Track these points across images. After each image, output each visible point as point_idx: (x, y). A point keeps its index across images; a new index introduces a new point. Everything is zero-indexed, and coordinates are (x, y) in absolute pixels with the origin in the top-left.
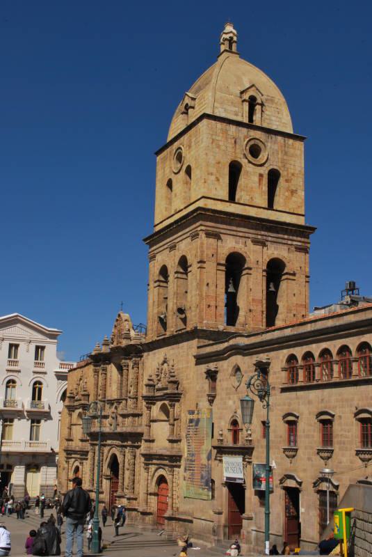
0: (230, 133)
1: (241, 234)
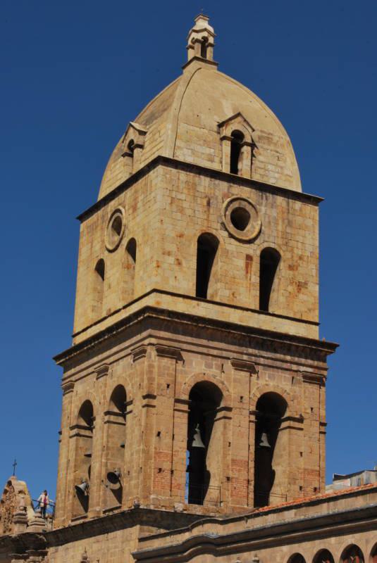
0: (201, 189)
1: (215, 352)
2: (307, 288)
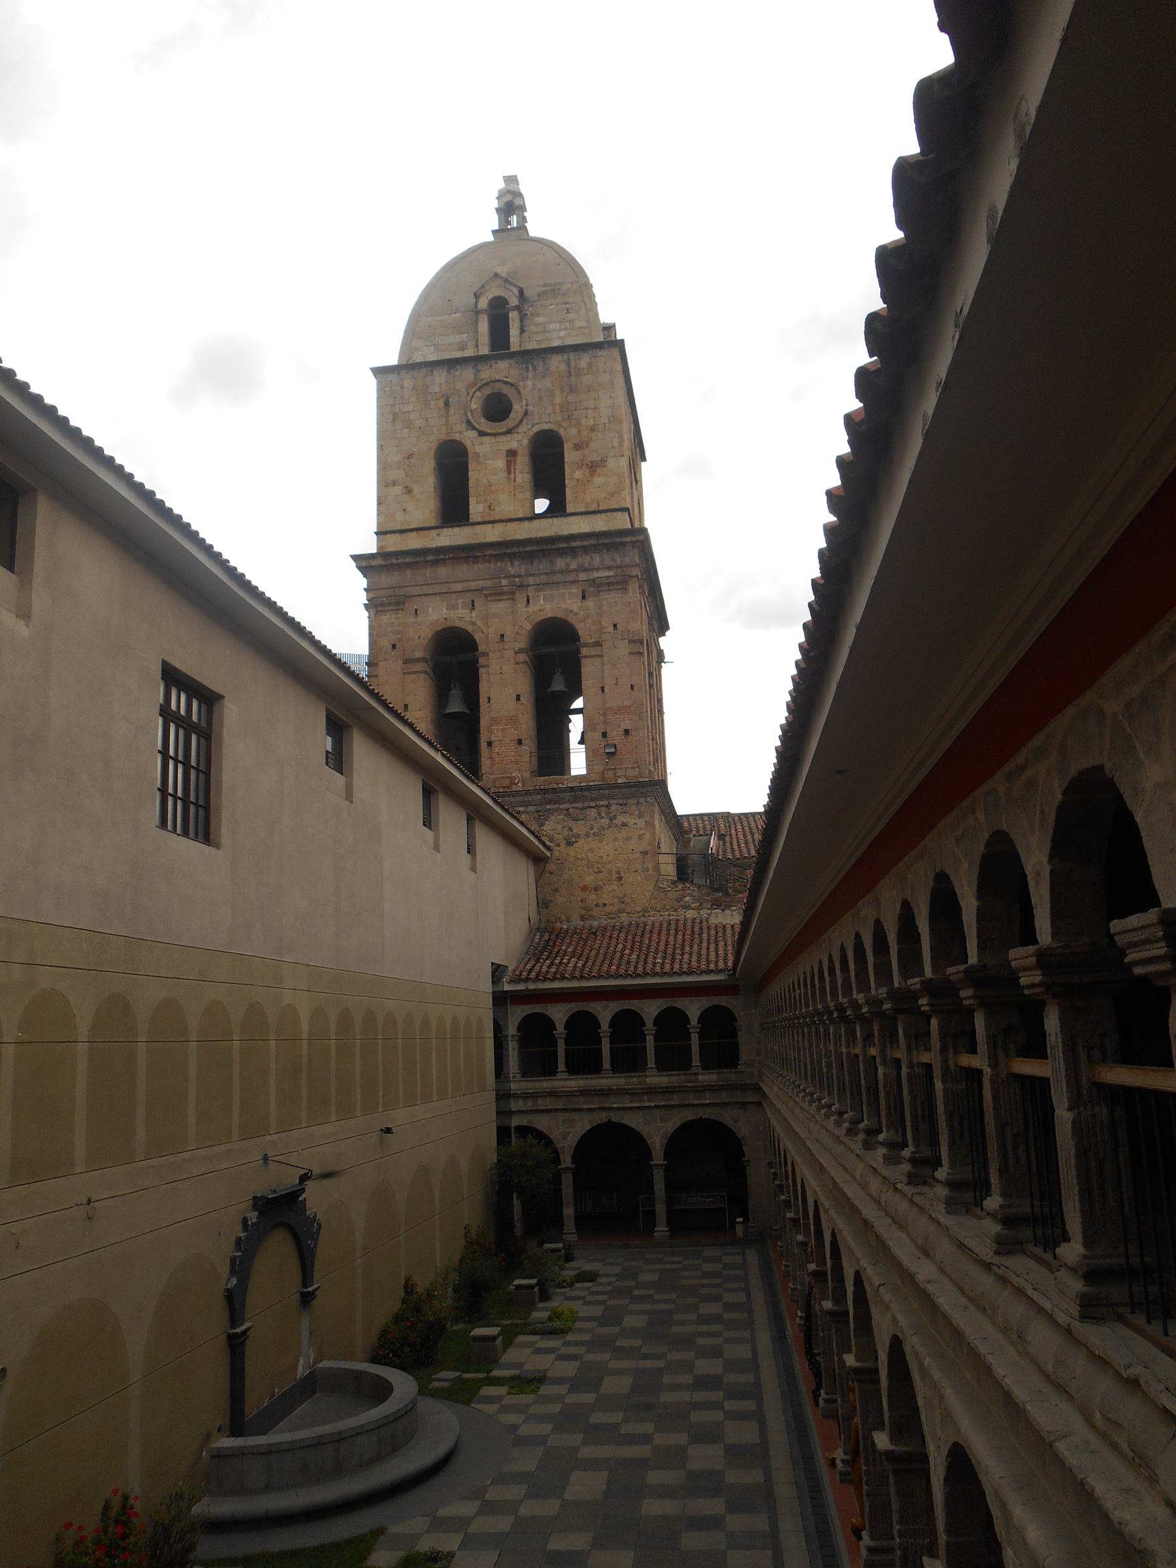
1: (459, 587)
2: (606, 466)
